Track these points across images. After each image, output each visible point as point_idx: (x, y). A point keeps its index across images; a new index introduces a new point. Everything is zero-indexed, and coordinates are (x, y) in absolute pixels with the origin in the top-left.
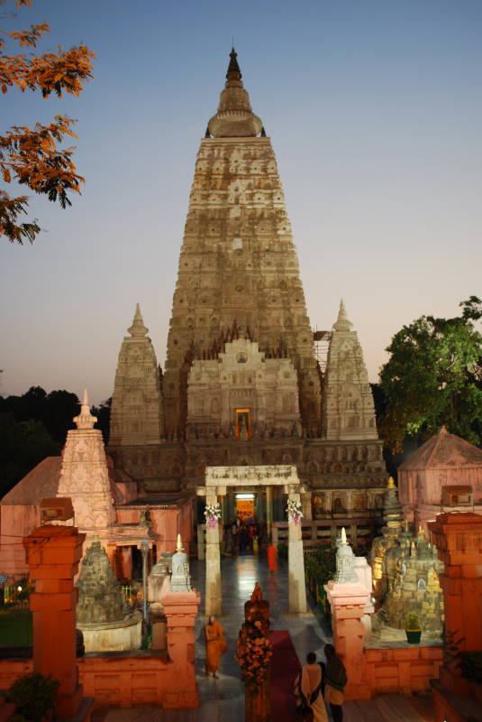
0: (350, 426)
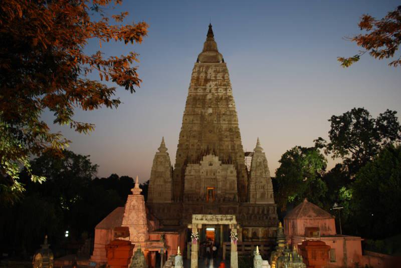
0: (261, 197)
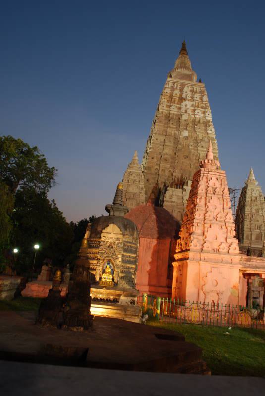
0: (256, 239)
